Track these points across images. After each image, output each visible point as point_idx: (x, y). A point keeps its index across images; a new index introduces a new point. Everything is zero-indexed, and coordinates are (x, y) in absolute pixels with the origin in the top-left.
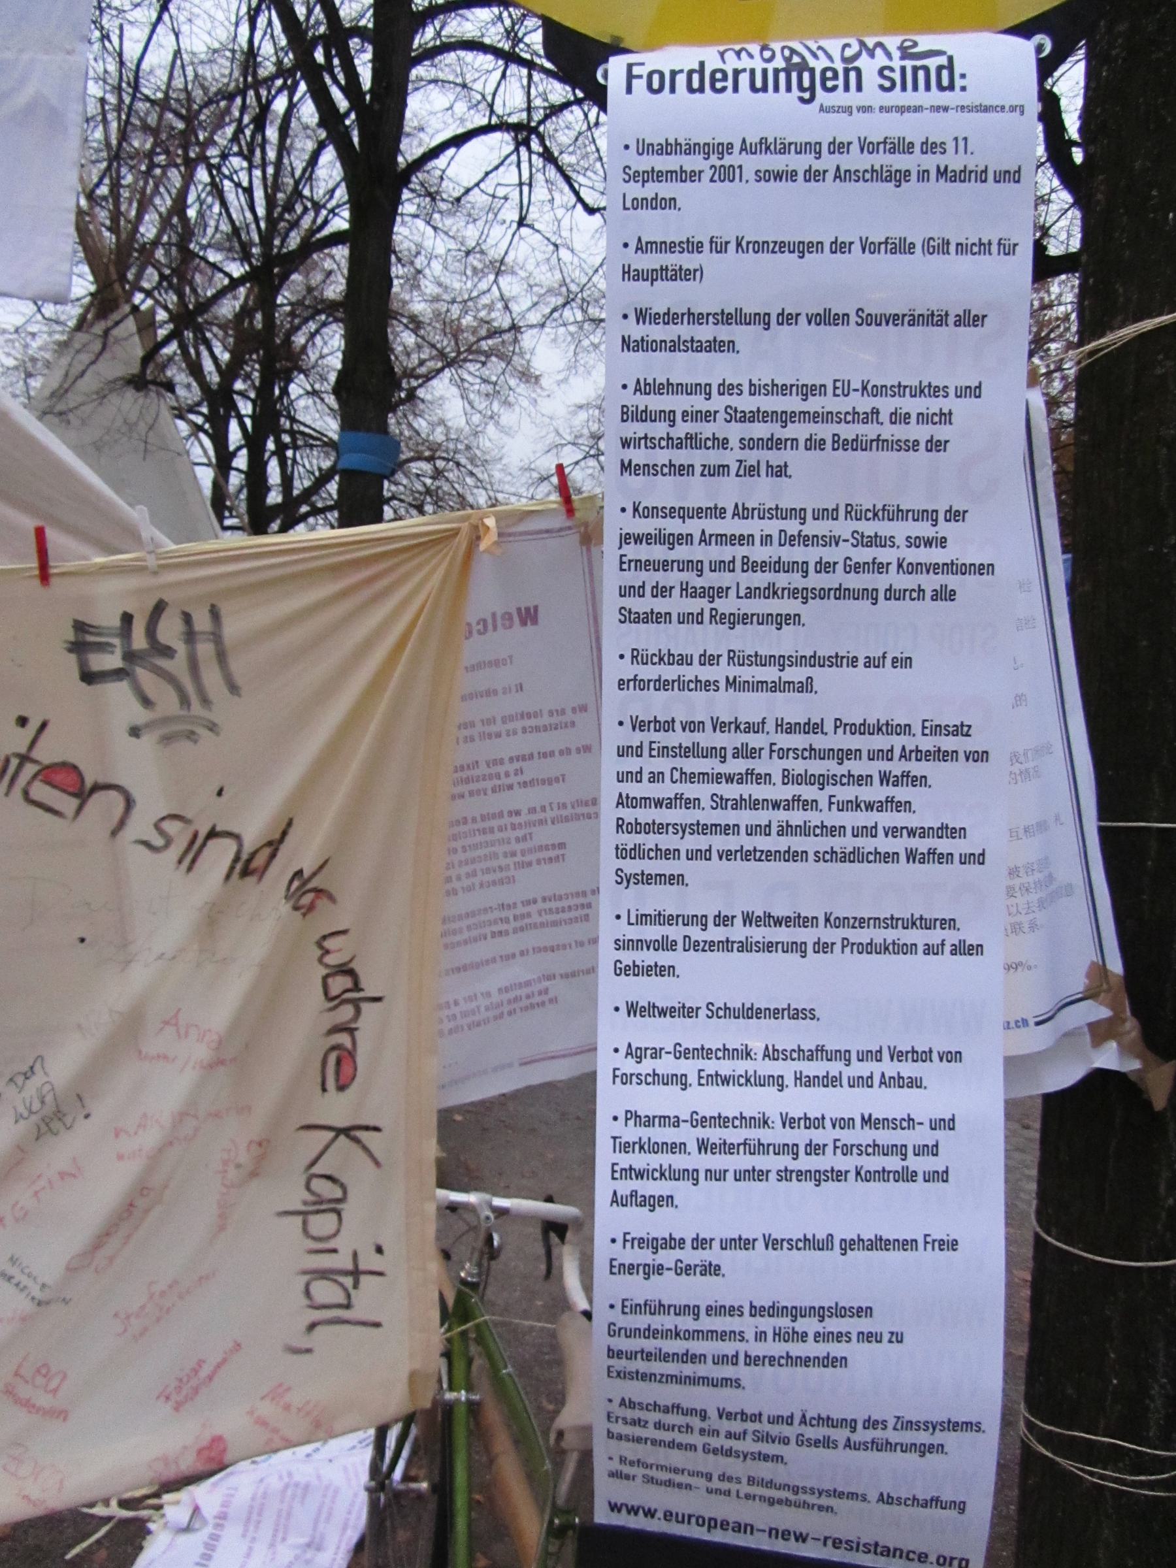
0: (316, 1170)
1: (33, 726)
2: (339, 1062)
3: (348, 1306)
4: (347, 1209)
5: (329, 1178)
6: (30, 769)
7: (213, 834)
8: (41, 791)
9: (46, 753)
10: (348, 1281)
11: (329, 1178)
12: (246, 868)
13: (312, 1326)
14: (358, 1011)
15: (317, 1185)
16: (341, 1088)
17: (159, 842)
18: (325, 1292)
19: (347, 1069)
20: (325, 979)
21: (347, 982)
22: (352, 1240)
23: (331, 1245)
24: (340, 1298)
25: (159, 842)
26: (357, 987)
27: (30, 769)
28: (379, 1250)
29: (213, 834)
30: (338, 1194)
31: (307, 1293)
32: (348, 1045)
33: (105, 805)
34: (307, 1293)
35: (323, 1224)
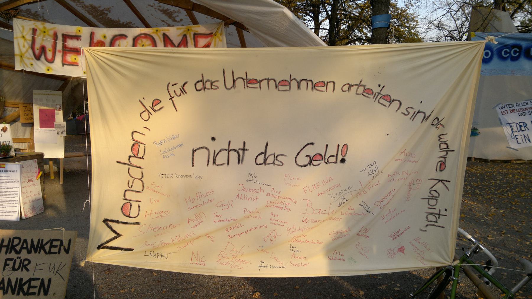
0: (433, 189)
1: (382, 86)
2: (441, 165)
3: (436, 222)
4: (439, 199)
5: (436, 191)
6: (380, 96)
7: (419, 112)
8: (382, 101)
9: (384, 93)
10: (437, 216)
11: (436, 191)
12: (425, 118)
13: (427, 225)
14: (447, 153)
15: (433, 192)
16: (441, 171)
17: (406, 113)
18: (431, 218)
19: (443, 166)
20: (440, 144)
21: (445, 146)
22: (440, 206)
23: (434, 207)
24: (435, 220)
25: (406, 113)
26: (448, 148)
27: (380, 96)
28: (446, 210)
29: (419, 112)
30: (437, 196)
31: (427, 217)
32: (444, 161)
33: (396, 104)
34: (427, 217)
35: (433, 202)
